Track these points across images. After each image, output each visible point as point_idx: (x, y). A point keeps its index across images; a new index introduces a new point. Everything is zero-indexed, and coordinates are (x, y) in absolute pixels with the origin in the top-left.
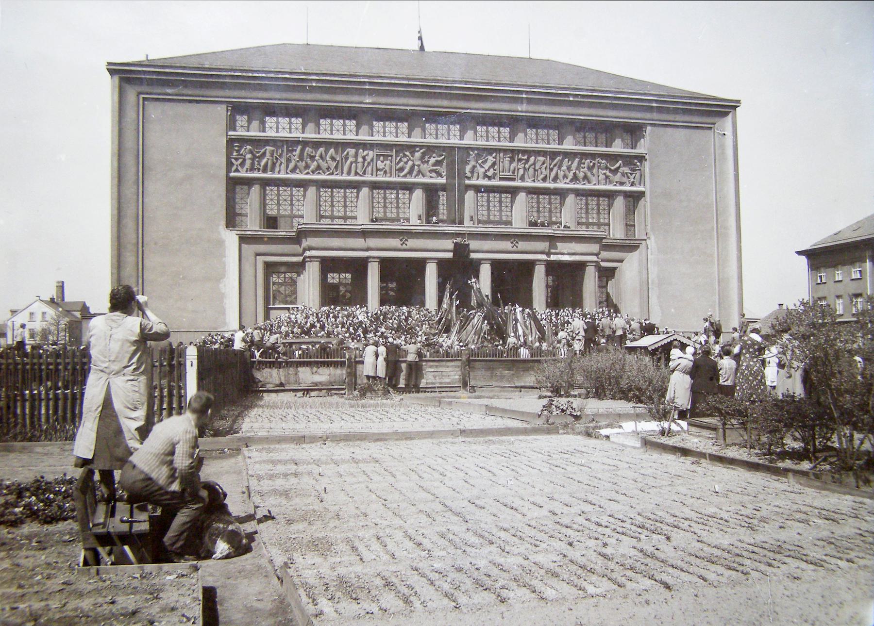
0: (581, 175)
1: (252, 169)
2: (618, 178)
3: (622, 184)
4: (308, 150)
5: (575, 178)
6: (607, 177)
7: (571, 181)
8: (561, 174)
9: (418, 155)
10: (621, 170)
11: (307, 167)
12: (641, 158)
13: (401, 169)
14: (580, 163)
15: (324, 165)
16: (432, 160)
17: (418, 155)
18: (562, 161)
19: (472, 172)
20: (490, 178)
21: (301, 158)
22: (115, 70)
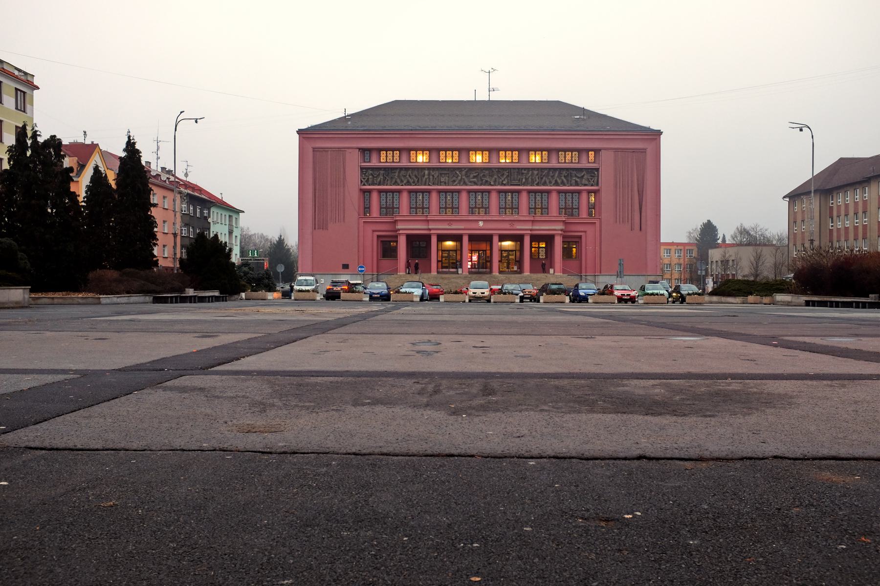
0: (559, 181)
1: (373, 184)
2: (584, 181)
3: (585, 185)
4: (403, 172)
5: (556, 184)
6: (576, 182)
7: (554, 185)
8: (548, 181)
9: (464, 173)
10: (585, 177)
11: (402, 181)
12: (597, 170)
13: (454, 181)
14: (560, 174)
15: (411, 181)
16: (472, 176)
17: (464, 173)
18: (548, 173)
19: (495, 181)
20: (505, 185)
21: (399, 176)
22: (300, 132)
